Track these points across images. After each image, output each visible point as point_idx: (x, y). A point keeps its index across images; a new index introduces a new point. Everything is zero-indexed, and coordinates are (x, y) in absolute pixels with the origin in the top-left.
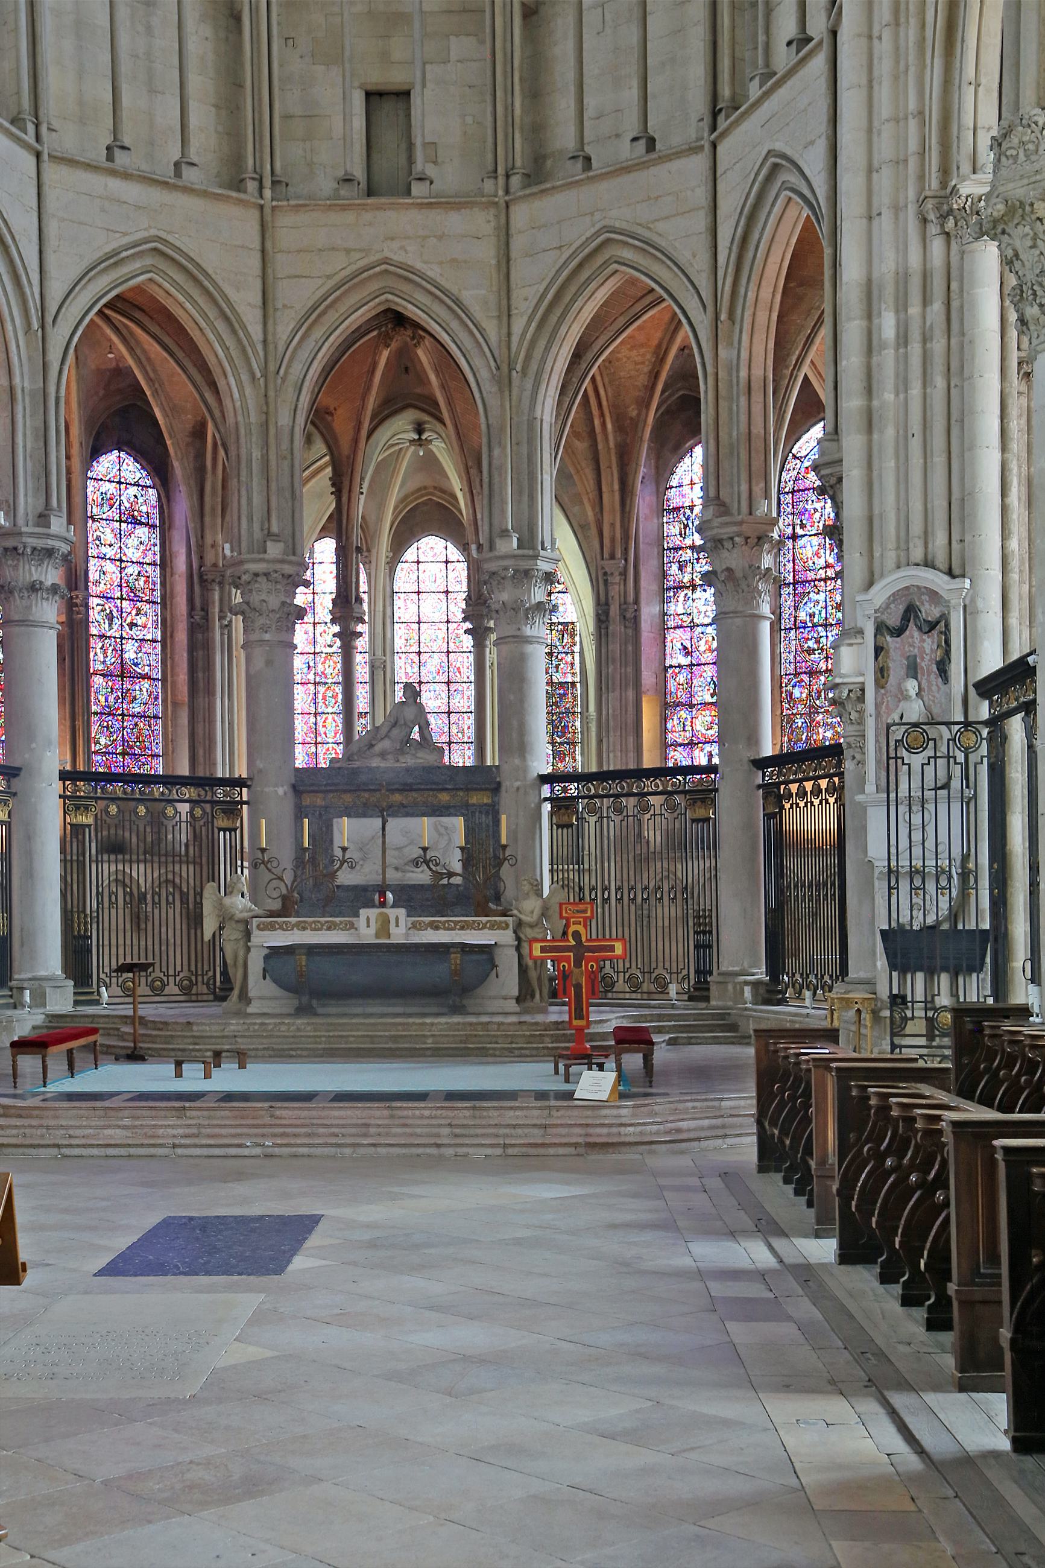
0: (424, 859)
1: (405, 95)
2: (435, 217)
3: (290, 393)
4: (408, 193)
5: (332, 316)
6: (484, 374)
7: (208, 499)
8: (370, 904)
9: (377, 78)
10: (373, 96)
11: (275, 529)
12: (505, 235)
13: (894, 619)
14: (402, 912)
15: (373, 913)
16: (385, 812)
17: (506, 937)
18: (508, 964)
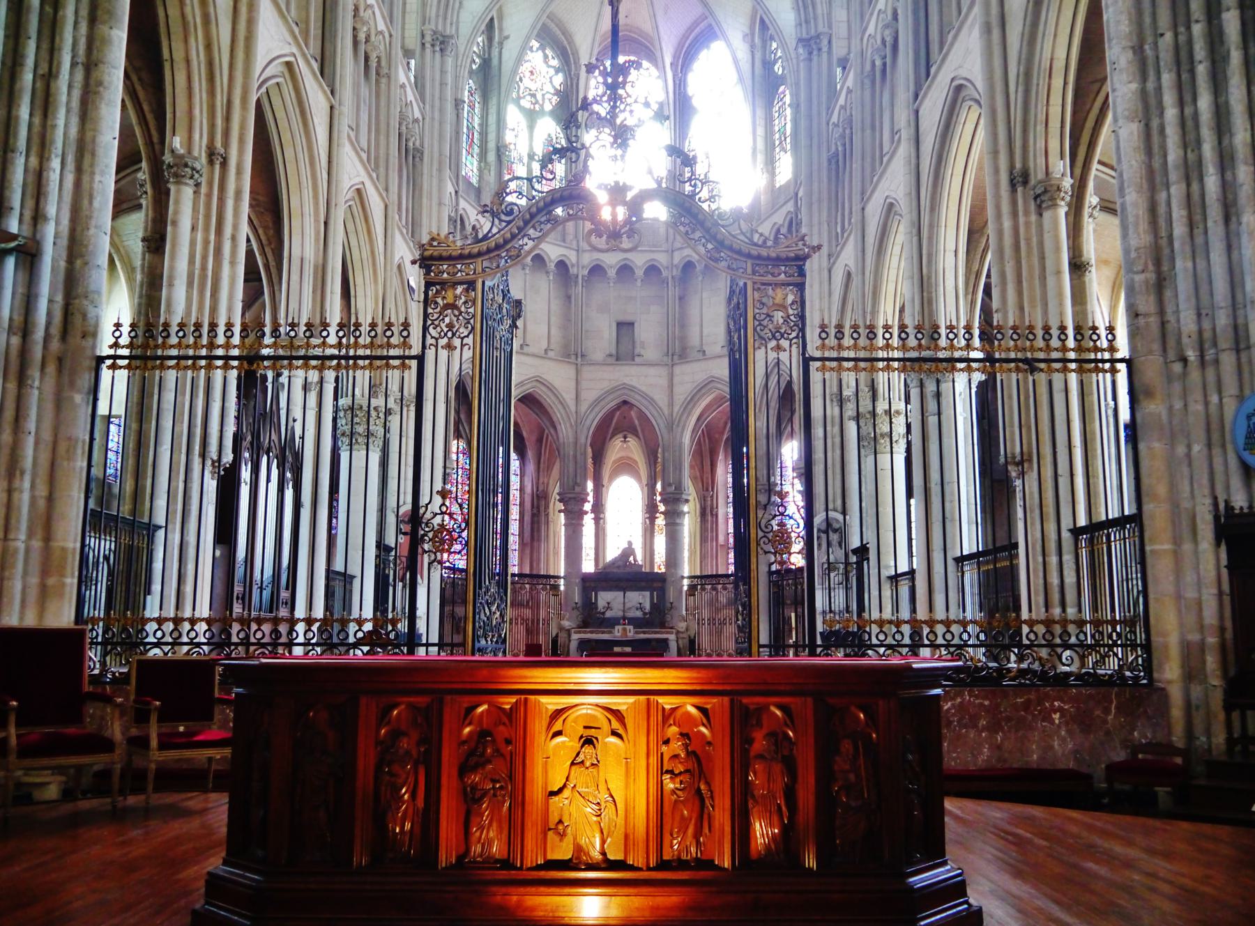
0: (641, 608)
1: (631, 324)
2: (644, 369)
3: (585, 431)
4: (633, 360)
5: (602, 403)
6: (662, 426)
7: (542, 465)
8: (619, 624)
9: (622, 318)
10: (620, 325)
11: (578, 481)
12: (671, 377)
13: (824, 527)
14: (632, 627)
15: (620, 627)
16: (624, 590)
17: (672, 637)
18: (673, 646)
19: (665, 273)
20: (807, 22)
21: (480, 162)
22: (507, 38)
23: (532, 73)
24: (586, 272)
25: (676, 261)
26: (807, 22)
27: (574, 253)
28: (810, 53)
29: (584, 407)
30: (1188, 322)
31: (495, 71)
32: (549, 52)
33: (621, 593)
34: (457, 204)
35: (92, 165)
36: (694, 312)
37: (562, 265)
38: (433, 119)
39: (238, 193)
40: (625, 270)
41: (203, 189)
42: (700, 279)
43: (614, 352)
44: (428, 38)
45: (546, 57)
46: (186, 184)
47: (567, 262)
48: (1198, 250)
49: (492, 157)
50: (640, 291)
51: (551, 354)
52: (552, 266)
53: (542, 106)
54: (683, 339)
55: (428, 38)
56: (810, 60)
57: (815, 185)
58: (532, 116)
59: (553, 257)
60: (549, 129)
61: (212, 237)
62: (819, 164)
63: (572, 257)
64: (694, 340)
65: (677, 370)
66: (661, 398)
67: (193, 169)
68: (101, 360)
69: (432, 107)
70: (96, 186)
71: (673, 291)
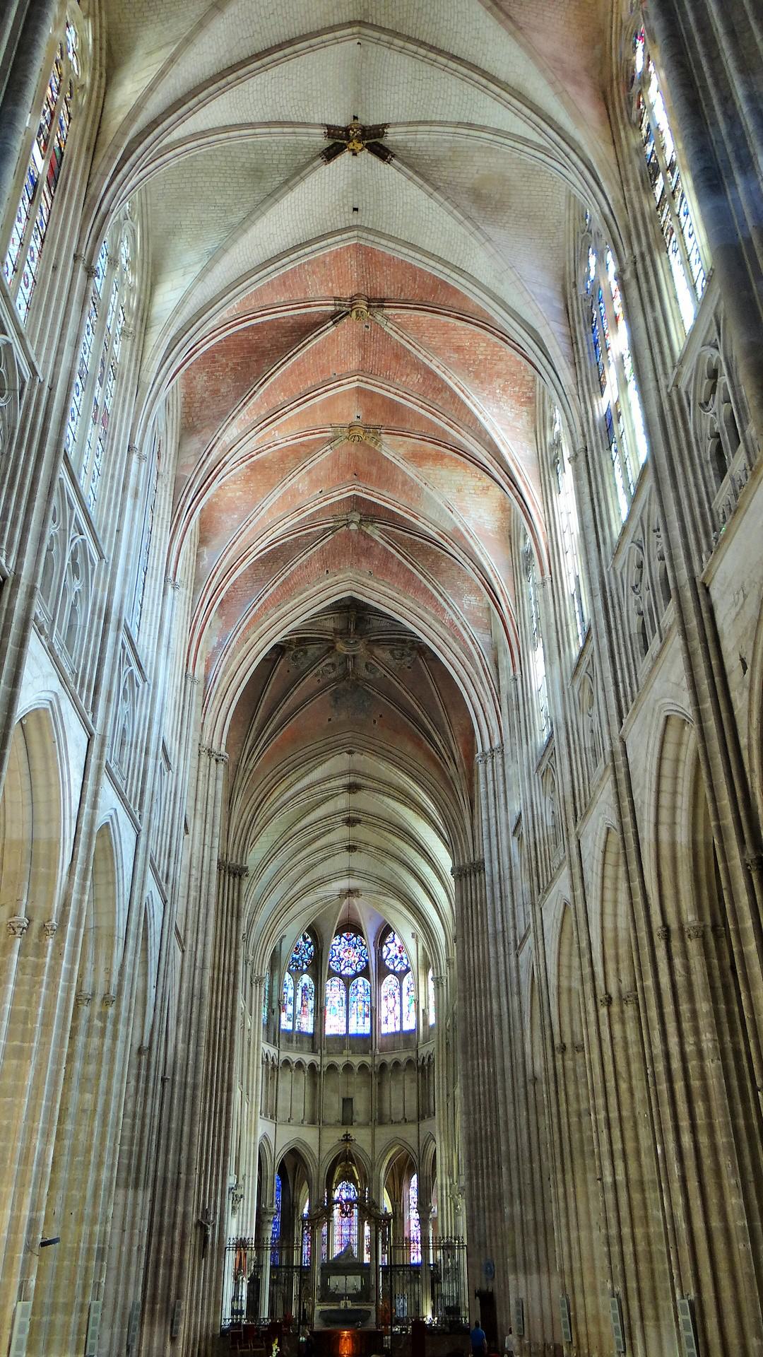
12: (373, 1136)
17: (373, 1308)
19: (370, 1069)
29: (323, 1155)
30: (476, 1236)
33: (344, 1277)
36: (386, 1093)
37: (312, 1066)
40: (348, 1067)
43: (341, 1119)
45: (305, 939)
48: (479, 1220)
49: (275, 1006)
50: (356, 1079)
51: (305, 1122)
54: (381, 1110)
58: (296, 974)
60: (306, 979)
63: (317, 1059)
64: (387, 1111)
65: (379, 1130)
66: (368, 1149)
71: (375, 1081)
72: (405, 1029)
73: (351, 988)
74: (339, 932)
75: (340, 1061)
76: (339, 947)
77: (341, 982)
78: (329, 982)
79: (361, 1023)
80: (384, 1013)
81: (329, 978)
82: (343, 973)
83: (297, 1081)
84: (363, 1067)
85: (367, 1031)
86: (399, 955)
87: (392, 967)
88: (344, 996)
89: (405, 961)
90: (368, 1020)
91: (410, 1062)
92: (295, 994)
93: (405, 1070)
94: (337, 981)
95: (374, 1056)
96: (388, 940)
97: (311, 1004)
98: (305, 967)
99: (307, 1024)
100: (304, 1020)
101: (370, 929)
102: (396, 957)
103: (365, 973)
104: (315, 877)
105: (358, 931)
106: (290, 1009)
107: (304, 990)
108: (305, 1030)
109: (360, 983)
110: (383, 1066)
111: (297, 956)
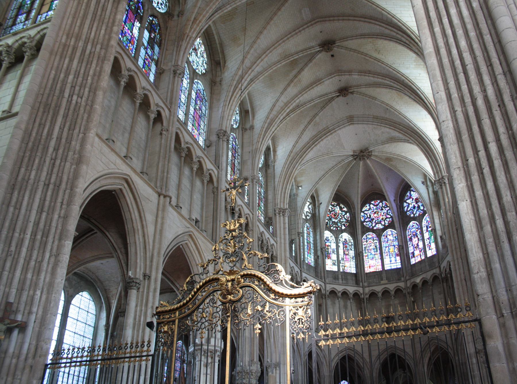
19: (404, 292)
20: (437, 173)
21: (314, 256)
22: (321, 203)
23: (335, 215)
24: (368, 296)
25: (408, 285)
26: (437, 173)
27: (362, 289)
28: (441, 185)
31: (317, 218)
32: (343, 206)
34: (301, 275)
35: (52, 291)
37: (356, 295)
38: (281, 243)
39: (155, 289)
40: (386, 292)
41: (141, 290)
42: (420, 291)
44: (277, 211)
46: (134, 289)
47: (358, 293)
49: (319, 253)
52: (351, 296)
53: (341, 228)
55: (277, 211)
56: (442, 188)
57: (453, 241)
58: (337, 233)
59: (351, 292)
60: (346, 236)
61: (143, 308)
62: (453, 232)
63: (361, 290)
67: (136, 283)
68: (47, 365)
69: (281, 238)
70: (53, 298)
72: (428, 256)
73: (383, 238)
74: (366, 200)
75: (379, 289)
76: (370, 212)
77: (374, 235)
78: (364, 237)
79: (393, 261)
80: (411, 250)
81: (363, 233)
82: (375, 228)
83: (346, 307)
84: (398, 291)
85: (399, 266)
86: (416, 205)
87: (412, 215)
88: (378, 244)
89: (422, 208)
90: (398, 258)
91: (435, 278)
92: (338, 247)
93: (432, 285)
94: (370, 235)
95: (406, 281)
96: (406, 198)
97: (352, 253)
98: (343, 228)
99: (350, 267)
100: (347, 264)
101: (390, 192)
102: (414, 207)
103: (391, 226)
104: (321, 128)
105: (382, 197)
106: (334, 257)
107: (345, 243)
108: (349, 271)
109: (390, 233)
110: (415, 286)
111: (336, 221)
